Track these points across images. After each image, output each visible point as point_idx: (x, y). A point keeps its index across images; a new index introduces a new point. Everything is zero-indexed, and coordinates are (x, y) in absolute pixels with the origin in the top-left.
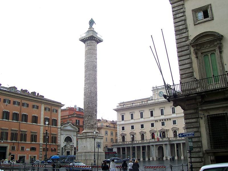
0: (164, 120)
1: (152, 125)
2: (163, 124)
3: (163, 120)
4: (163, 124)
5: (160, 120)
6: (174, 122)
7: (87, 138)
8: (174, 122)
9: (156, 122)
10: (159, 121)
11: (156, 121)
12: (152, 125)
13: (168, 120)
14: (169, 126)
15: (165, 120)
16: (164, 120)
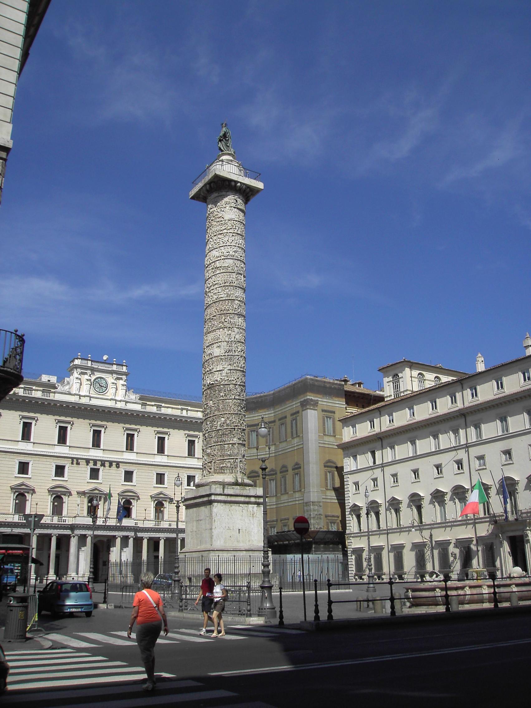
0: (99, 463)
1: (60, 471)
2: (94, 474)
3: (95, 462)
4: (94, 474)
5: (88, 461)
6: (129, 476)
7: (248, 503)
8: (129, 476)
9: (72, 463)
10: (83, 463)
11: (76, 461)
12: (60, 471)
13: (111, 463)
14: (112, 482)
15: (103, 465)
16: (99, 463)
